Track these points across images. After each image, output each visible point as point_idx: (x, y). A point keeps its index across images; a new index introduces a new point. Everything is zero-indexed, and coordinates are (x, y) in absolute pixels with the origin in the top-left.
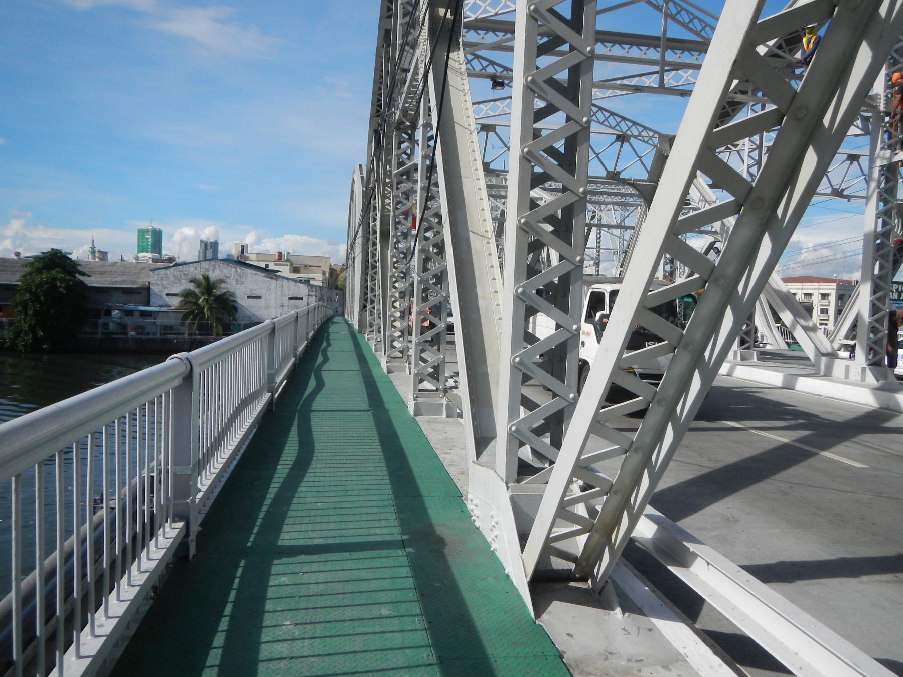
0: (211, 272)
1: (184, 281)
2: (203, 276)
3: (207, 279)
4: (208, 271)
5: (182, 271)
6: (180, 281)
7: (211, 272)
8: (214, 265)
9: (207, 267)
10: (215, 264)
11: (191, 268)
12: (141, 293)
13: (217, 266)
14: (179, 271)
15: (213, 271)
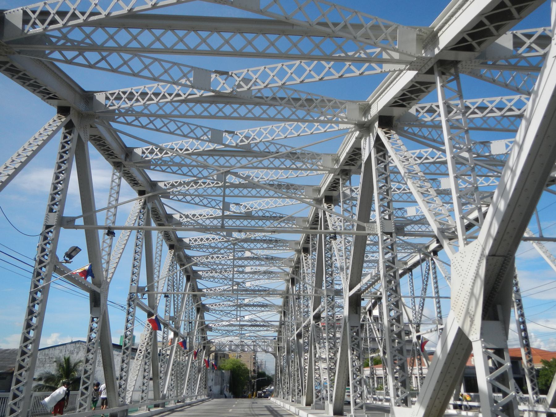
0: (75, 354)
1: (48, 365)
2: (65, 358)
3: (68, 361)
4: (73, 353)
5: (48, 355)
6: (44, 364)
7: (75, 354)
8: (79, 347)
9: (72, 349)
10: (79, 347)
11: (57, 352)
12: (4, 378)
13: (81, 349)
14: (45, 355)
15: (78, 353)
